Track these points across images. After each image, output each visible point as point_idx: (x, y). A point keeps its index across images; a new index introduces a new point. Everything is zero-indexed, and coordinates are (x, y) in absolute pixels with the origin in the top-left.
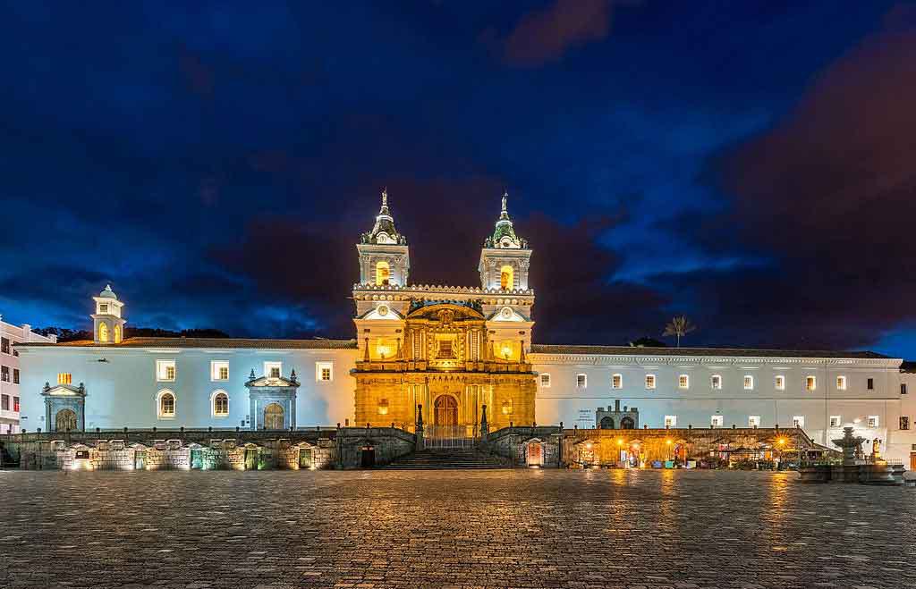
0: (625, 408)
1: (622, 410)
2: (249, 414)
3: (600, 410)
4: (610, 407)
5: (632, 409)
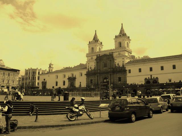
0: (154, 77)
1: (153, 78)
2: (68, 84)
3: (146, 79)
4: (149, 78)
5: (156, 78)
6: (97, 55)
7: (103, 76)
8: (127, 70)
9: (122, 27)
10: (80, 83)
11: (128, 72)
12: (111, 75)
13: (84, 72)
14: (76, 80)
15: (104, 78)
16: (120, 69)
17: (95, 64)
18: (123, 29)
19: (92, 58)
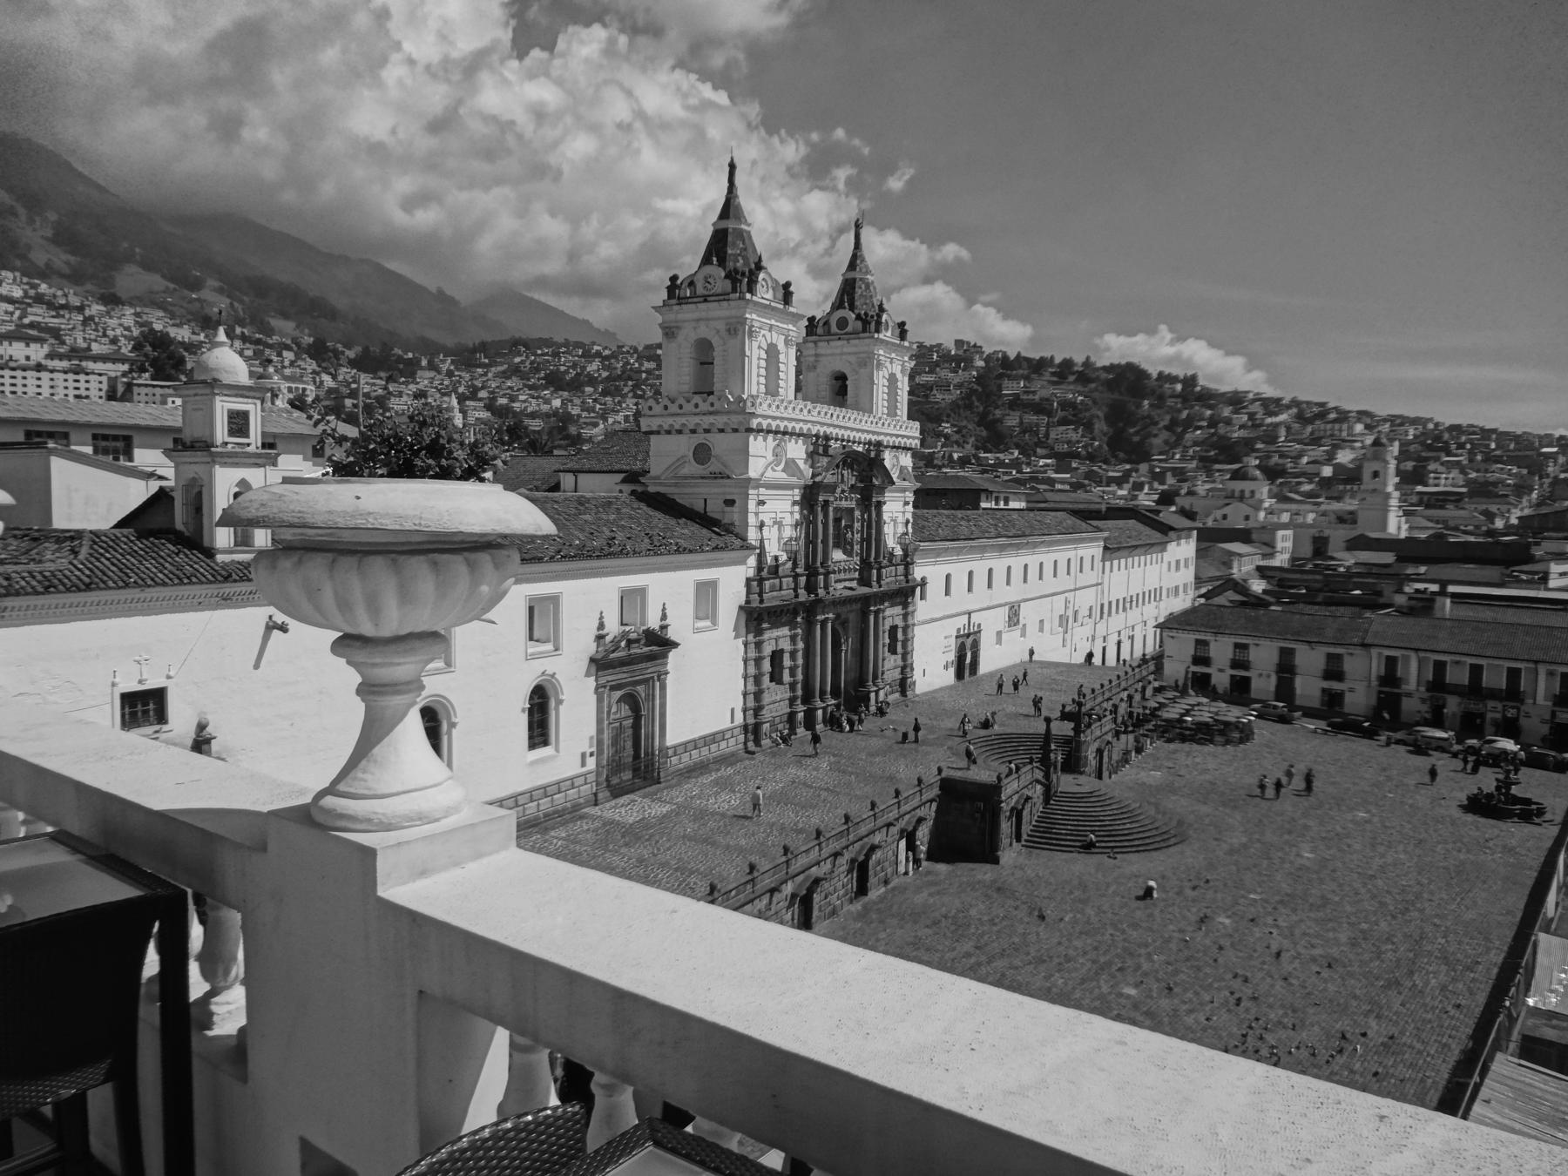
2: (593, 731)
13: (732, 580)
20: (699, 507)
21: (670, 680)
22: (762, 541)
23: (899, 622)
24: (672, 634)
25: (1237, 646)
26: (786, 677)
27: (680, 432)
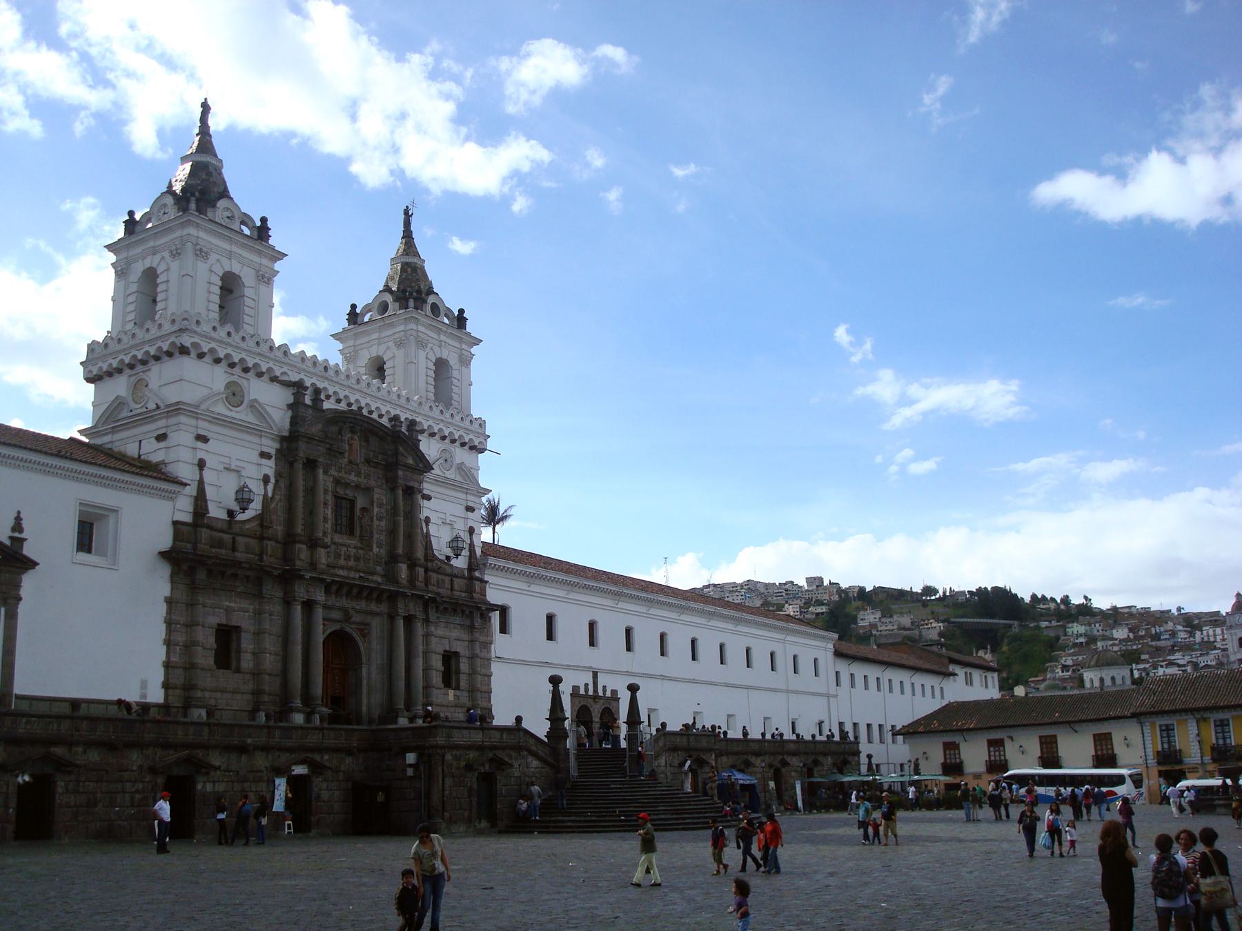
1: (601, 693)
4: (586, 685)
6: (298, 387)
7: (336, 615)
8: (493, 607)
9: (408, 235)
10: (555, 681)
11: (495, 617)
12: (409, 620)
14: (29, 583)
15: (329, 631)
16: (456, 587)
17: (269, 467)
18: (417, 255)
19: (234, 395)
20: (131, 450)
21: (22, 609)
22: (201, 483)
23: (460, 648)
24: (27, 551)
25: (991, 743)
26: (247, 662)
27: (119, 371)
